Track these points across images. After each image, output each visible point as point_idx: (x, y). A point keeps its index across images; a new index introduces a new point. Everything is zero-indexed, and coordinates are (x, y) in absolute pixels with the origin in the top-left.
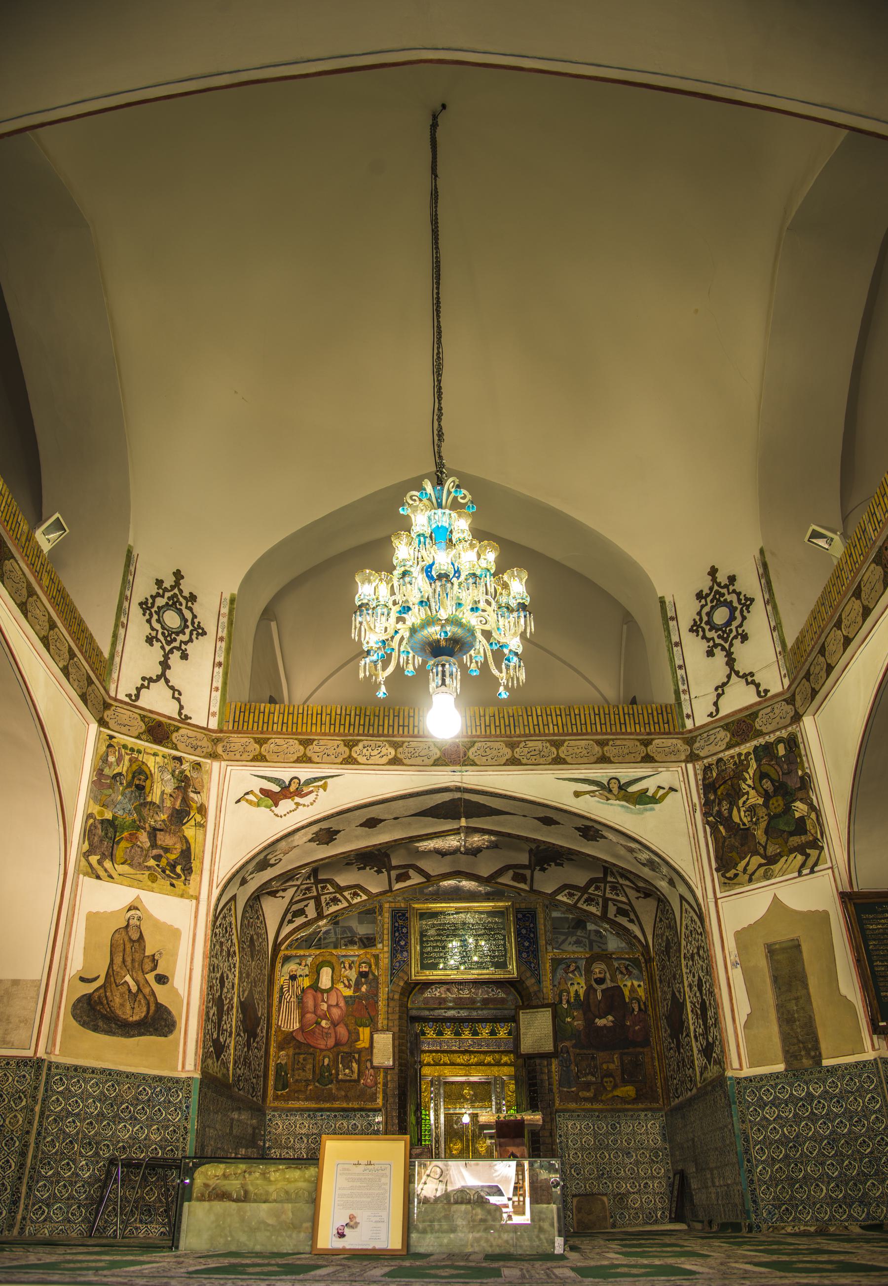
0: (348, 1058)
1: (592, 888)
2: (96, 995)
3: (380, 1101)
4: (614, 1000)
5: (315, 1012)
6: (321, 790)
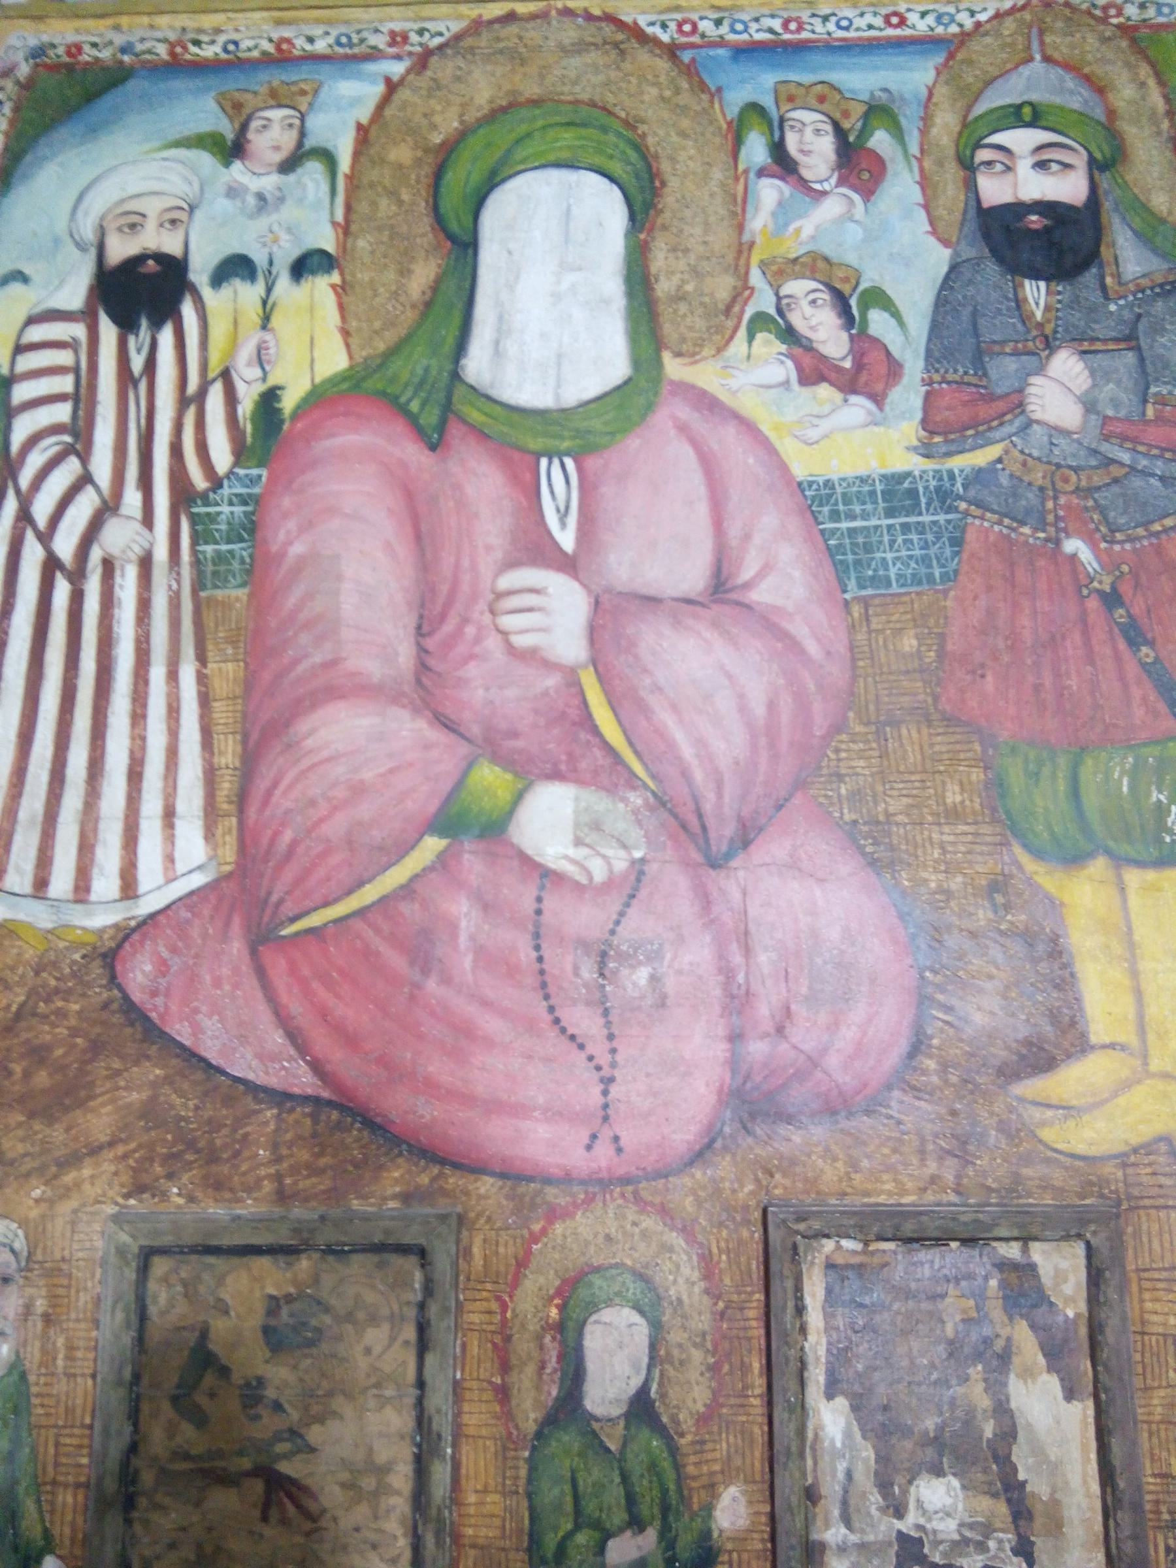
5: (427, 688)
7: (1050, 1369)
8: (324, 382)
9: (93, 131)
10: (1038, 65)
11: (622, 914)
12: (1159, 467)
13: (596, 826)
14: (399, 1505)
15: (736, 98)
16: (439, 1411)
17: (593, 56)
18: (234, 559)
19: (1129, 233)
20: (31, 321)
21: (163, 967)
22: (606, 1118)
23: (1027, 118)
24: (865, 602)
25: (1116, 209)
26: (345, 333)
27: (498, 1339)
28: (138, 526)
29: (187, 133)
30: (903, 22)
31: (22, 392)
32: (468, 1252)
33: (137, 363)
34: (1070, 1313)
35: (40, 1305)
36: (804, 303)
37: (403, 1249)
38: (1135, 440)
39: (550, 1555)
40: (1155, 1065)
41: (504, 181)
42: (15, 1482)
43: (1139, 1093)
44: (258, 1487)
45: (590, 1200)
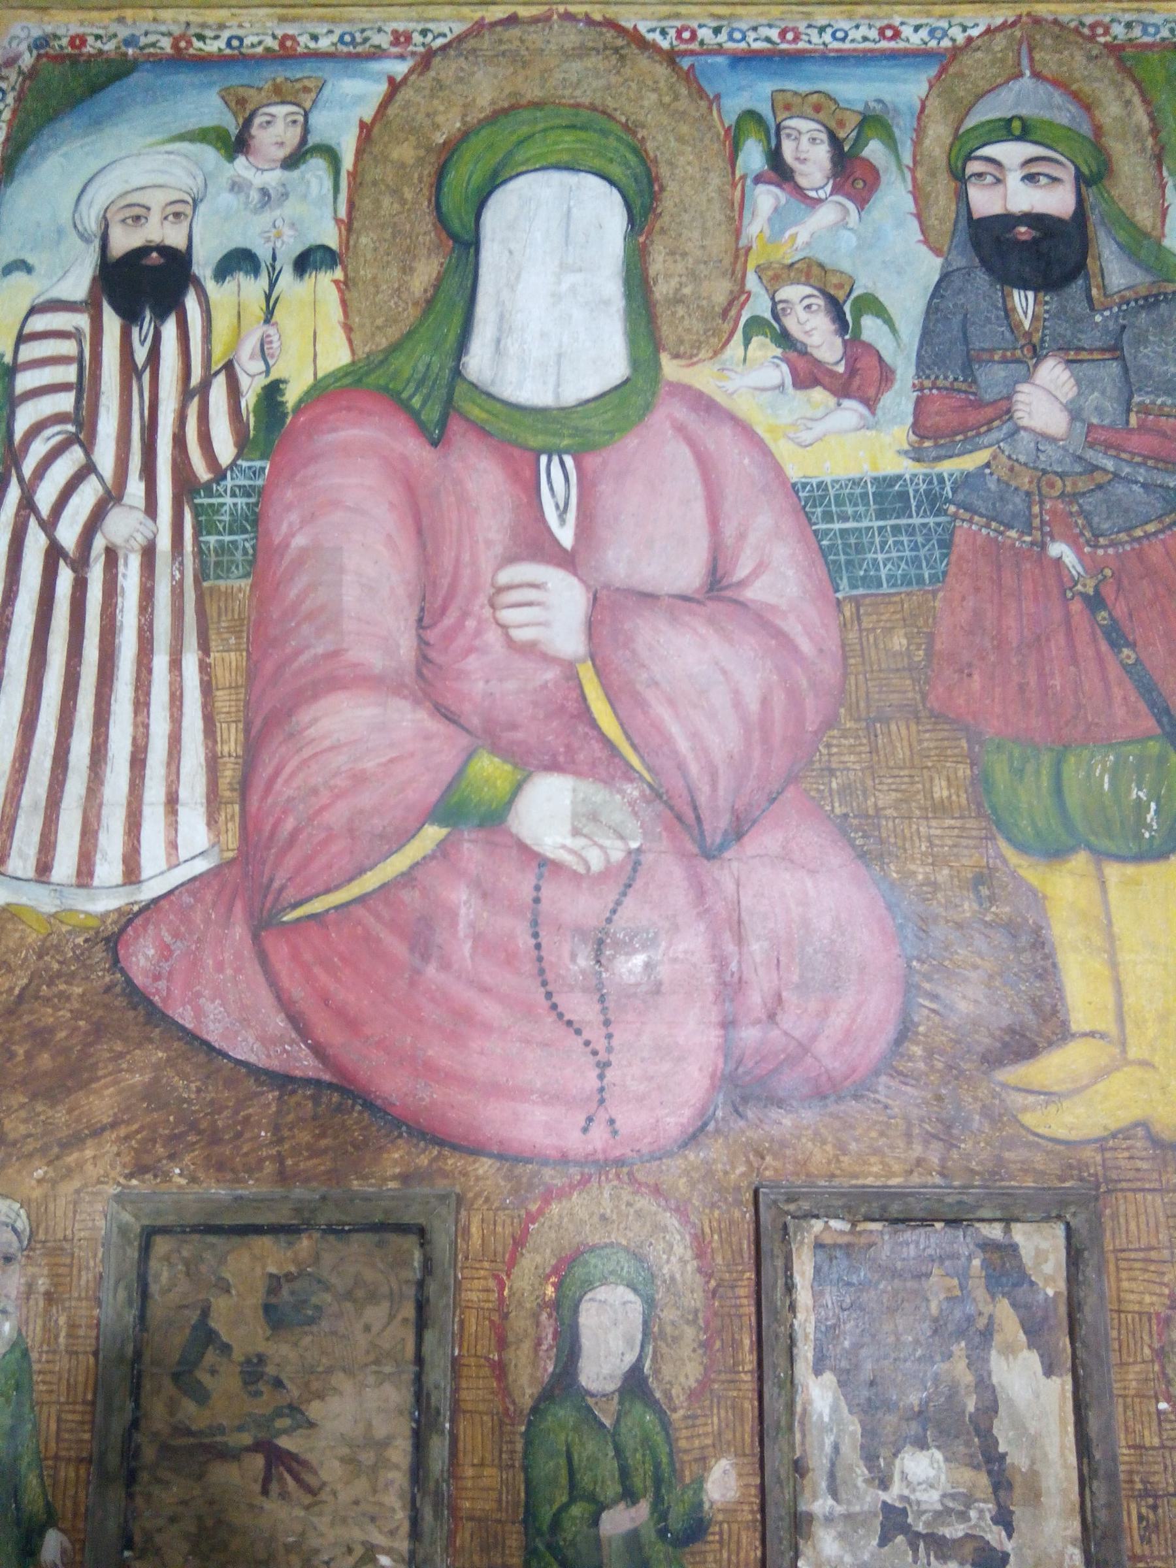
5: (428, 679)
7: (1030, 1346)
8: (325, 377)
9: (97, 123)
10: (1027, 81)
11: (618, 903)
12: (1142, 475)
13: (594, 817)
14: (398, 1478)
15: (733, 106)
16: (437, 1387)
17: (592, 61)
18: (236, 548)
19: (1115, 247)
20: (32, 311)
21: (165, 952)
22: (602, 1101)
23: (1017, 132)
24: (857, 601)
25: (1103, 224)
26: (348, 328)
27: (495, 1317)
28: (141, 516)
29: (190, 127)
30: (897, 35)
31: (25, 381)
32: (466, 1231)
33: (141, 354)
34: (1050, 1292)
35: (42, 1284)
36: (799, 309)
37: (402, 1229)
38: (1120, 448)
39: (545, 1528)
40: (1133, 1053)
41: (505, 182)
42: (17, 1458)
43: (1118, 1078)
44: (259, 1461)
45: (585, 1181)
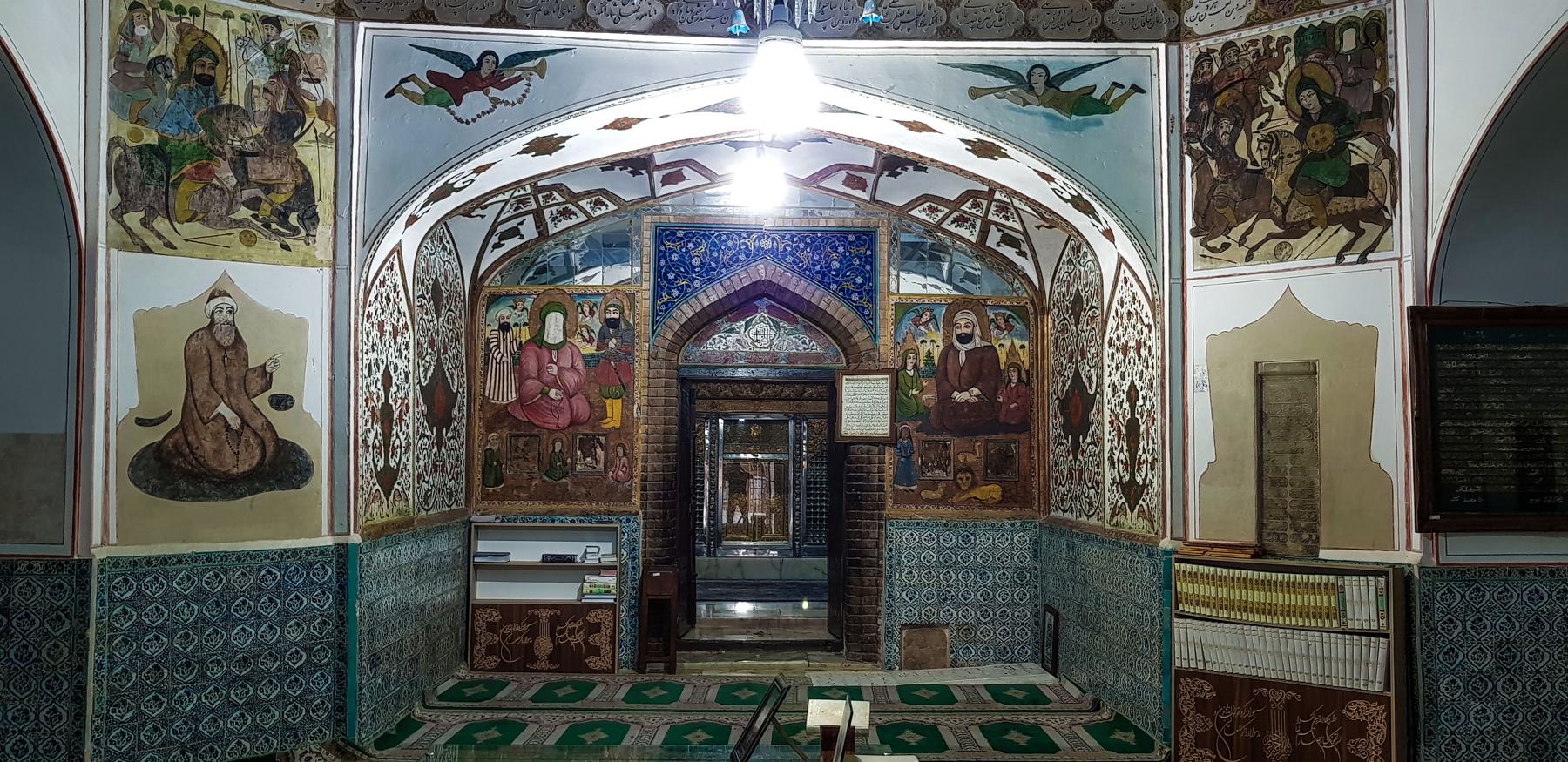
0: (588, 445)
1: (968, 204)
2: (170, 443)
3: (637, 500)
4: (984, 366)
5: (539, 378)
6: (536, 76)
